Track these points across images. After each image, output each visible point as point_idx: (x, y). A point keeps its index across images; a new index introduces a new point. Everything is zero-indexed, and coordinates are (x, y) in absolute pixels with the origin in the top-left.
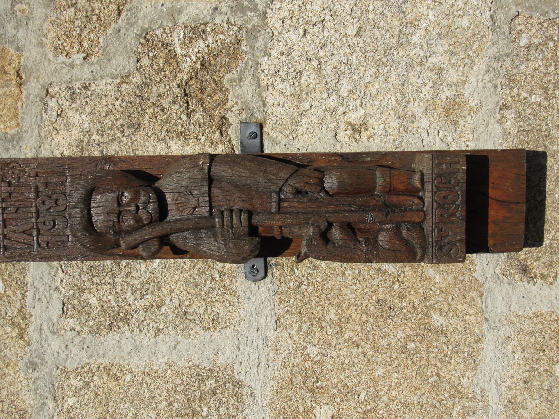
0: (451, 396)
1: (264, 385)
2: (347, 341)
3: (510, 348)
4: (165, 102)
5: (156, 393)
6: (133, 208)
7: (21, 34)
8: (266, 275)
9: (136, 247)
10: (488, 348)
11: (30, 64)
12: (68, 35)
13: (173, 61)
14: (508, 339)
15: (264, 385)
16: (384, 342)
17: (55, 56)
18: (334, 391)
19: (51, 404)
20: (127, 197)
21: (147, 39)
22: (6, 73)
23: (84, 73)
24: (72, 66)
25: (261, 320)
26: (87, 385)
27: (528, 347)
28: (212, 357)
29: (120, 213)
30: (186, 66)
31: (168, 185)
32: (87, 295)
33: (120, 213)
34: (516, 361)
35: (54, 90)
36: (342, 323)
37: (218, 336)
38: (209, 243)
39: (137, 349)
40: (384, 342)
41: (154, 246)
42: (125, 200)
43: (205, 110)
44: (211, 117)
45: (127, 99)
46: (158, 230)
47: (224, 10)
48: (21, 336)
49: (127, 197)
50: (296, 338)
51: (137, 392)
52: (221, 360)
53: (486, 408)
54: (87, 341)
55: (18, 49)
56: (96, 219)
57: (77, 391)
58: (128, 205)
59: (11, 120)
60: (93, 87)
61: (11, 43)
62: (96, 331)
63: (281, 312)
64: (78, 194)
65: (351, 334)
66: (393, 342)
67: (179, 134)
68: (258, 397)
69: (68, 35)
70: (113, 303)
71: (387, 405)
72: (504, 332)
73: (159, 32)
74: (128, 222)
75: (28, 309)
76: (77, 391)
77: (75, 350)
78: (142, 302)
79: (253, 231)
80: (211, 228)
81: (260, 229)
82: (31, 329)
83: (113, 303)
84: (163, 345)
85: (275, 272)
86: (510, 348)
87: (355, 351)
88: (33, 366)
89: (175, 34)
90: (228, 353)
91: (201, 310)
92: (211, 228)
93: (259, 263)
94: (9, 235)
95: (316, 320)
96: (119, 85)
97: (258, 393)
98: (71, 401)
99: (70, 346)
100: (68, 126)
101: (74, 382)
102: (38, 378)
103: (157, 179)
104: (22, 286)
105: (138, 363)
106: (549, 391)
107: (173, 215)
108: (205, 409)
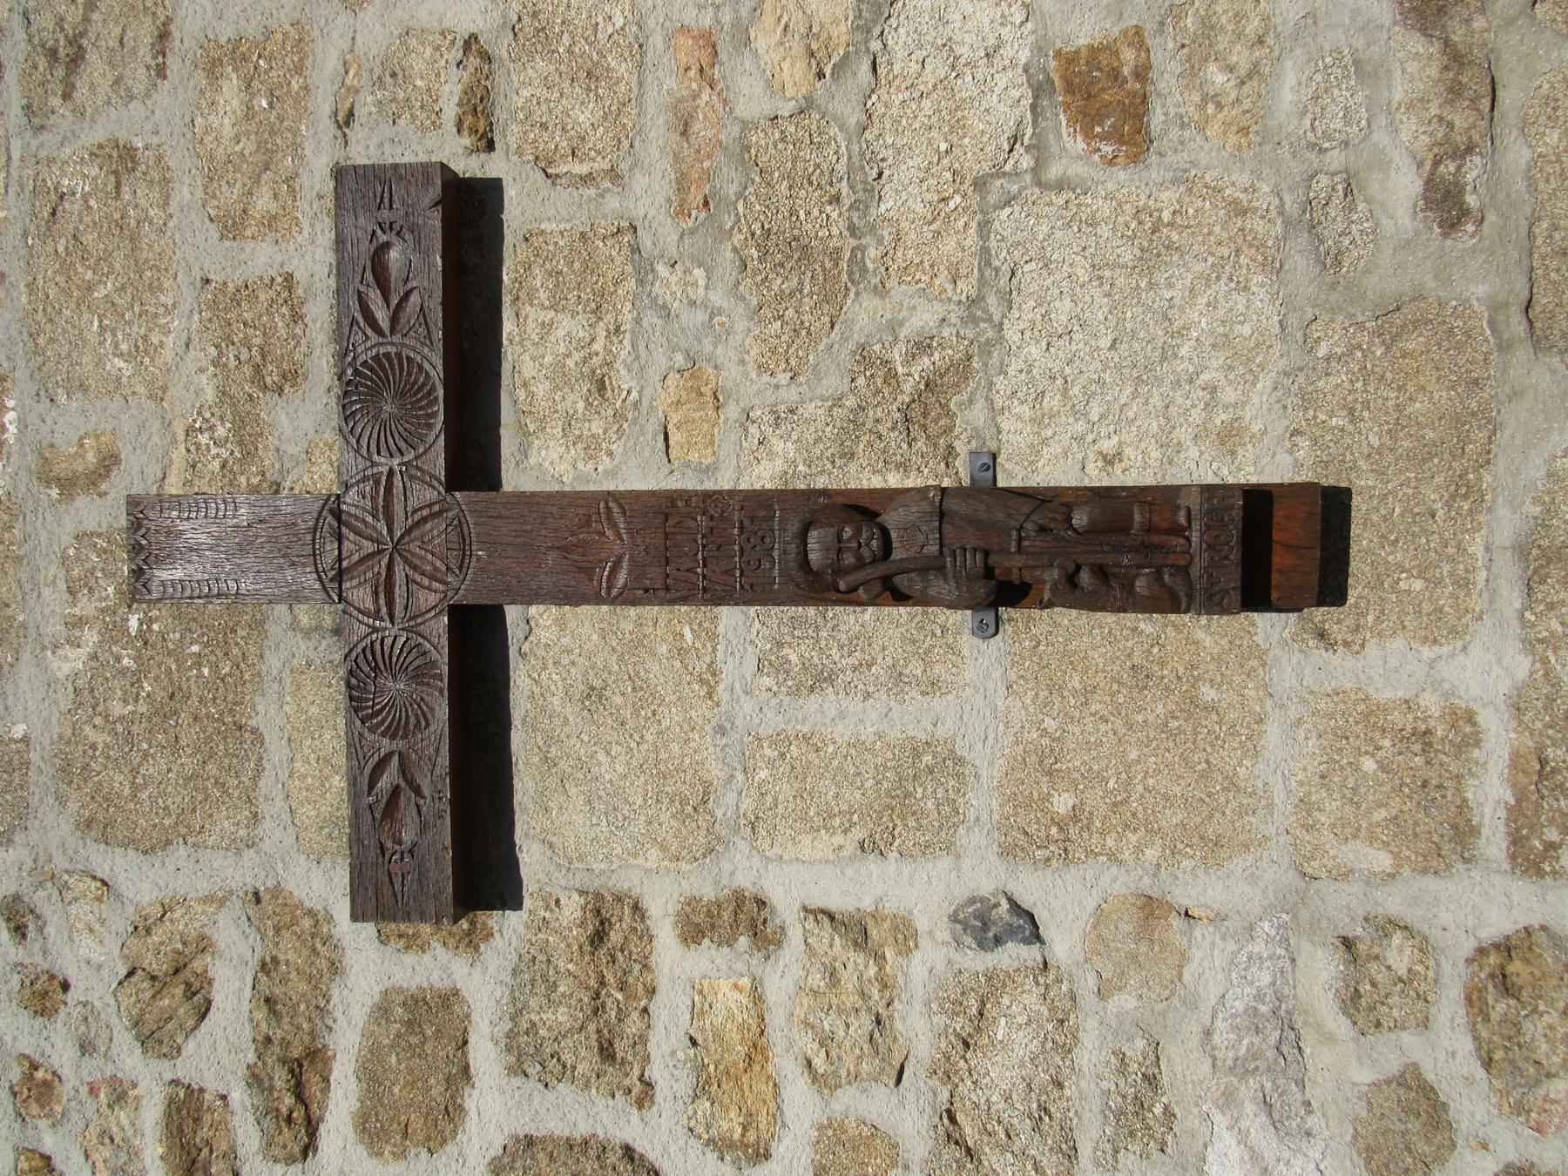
0: (1224, 789)
1: (991, 764)
2: (1094, 715)
3: (1301, 734)
4: (882, 429)
5: (863, 768)
6: (855, 545)
7: (719, 350)
8: (997, 632)
9: (855, 589)
10: (1273, 731)
11: (729, 385)
12: (773, 351)
13: (893, 382)
14: (1299, 722)
15: (991, 764)
16: (1140, 718)
17: (759, 375)
18: (1076, 775)
19: (740, 777)
20: (848, 532)
21: (863, 355)
22: (702, 394)
23: (791, 395)
24: (777, 387)
25: (990, 685)
26: (783, 755)
27: (1326, 732)
28: (930, 728)
29: (840, 551)
30: (907, 387)
31: (892, 519)
32: (786, 650)
33: (840, 551)
34: (1310, 749)
35: (755, 414)
36: (1088, 692)
37: (937, 703)
38: (939, 587)
39: (842, 715)
40: (1140, 718)
41: (877, 587)
42: (845, 536)
43: (928, 437)
44: (935, 445)
45: (838, 424)
46: (882, 569)
47: (953, 321)
48: (710, 695)
49: (848, 532)
50: (1031, 709)
51: (840, 768)
52: (941, 732)
53: (1270, 806)
54: (785, 705)
55: (716, 367)
56: (812, 556)
57: (770, 762)
58: (849, 540)
59: (706, 448)
60: (801, 411)
61: (709, 361)
62: (795, 692)
63: (1014, 677)
64: (794, 527)
65: (1099, 707)
66: (1151, 718)
67: (898, 466)
68: (984, 779)
69: (773, 351)
70: (816, 660)
71: (1142, 796)
72: (1293, 714)
73: (877, 348)
74: (849, 559)
75: (719, 664)
76: (770, 762)
77: (770, 714)
78: (850, 661)
79: (989, 573)
80: (941, 569)
81: (997, 571)
82: (721, 688)
83: (816, 660)
84: (873, 711)
85: (1008, 629)
86: (1301, 734)
87: (1103, 727)
88: (721, 730)
89: (896, 350)
90: (949, 723)
91: (919, 672)
92: (941, 569)
93: (989, 617)
94: (710, 575)
95: (1056, 687)
96: (831, 409)
97: (984, 773)
98: (763, 774)
99: (765, 709)
100: (771, 455)
101: (768, 752)
102: (726, 745)
103: (877, 515)
104: (713, 637)
105: (842, 733)
106: (1355, 790)
107: (897, 555)
108: (920, 790)
